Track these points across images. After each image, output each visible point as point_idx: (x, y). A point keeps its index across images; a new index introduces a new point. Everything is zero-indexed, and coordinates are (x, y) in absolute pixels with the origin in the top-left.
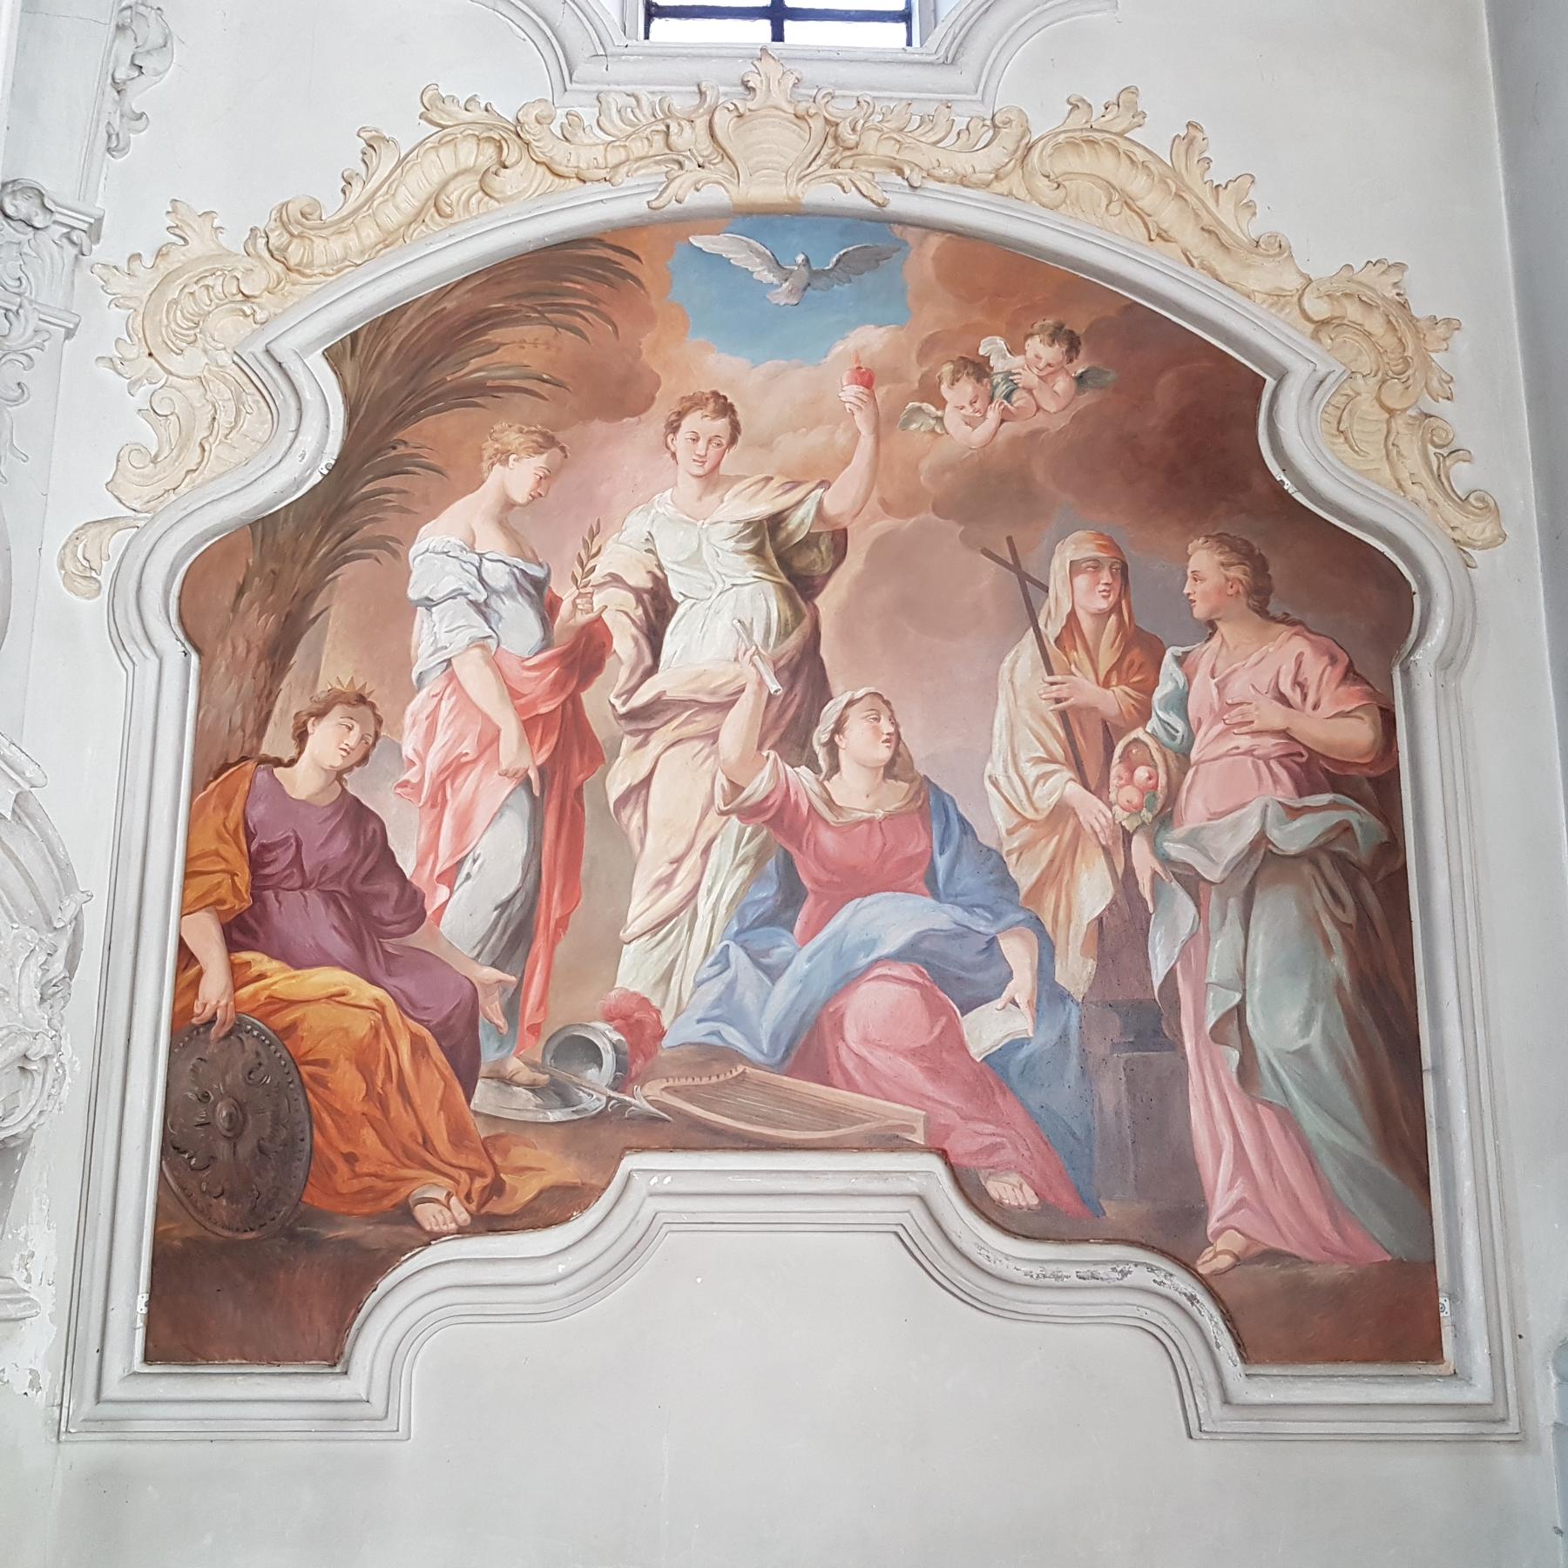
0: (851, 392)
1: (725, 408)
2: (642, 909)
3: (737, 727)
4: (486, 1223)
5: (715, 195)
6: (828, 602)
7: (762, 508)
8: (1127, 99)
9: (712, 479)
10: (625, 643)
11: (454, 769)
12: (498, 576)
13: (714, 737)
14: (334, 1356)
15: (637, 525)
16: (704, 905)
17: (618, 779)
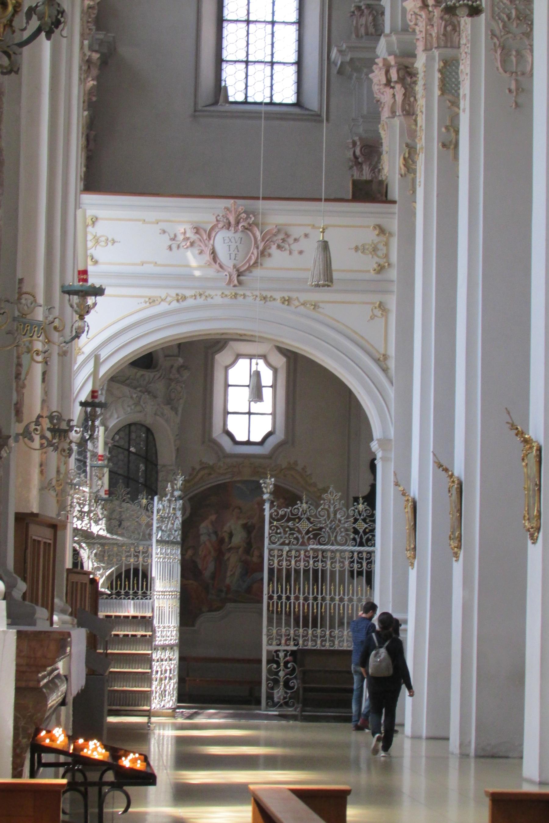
0: (256, 506)
1: (240, 508)
2: (229, 574)
3: (241, 550)
4: (210, 610)
5: (238, 479)
6: (253, 535)
7: (245, 522)
8: (296, 463)
9: (238, 518)
10: (227, 540)
11: (205, 556)
12: (211, 531)
13: (238, 552)
14: (193, 625)
15: (228, 525)
16: (236, 574)
17: (226, 557)
